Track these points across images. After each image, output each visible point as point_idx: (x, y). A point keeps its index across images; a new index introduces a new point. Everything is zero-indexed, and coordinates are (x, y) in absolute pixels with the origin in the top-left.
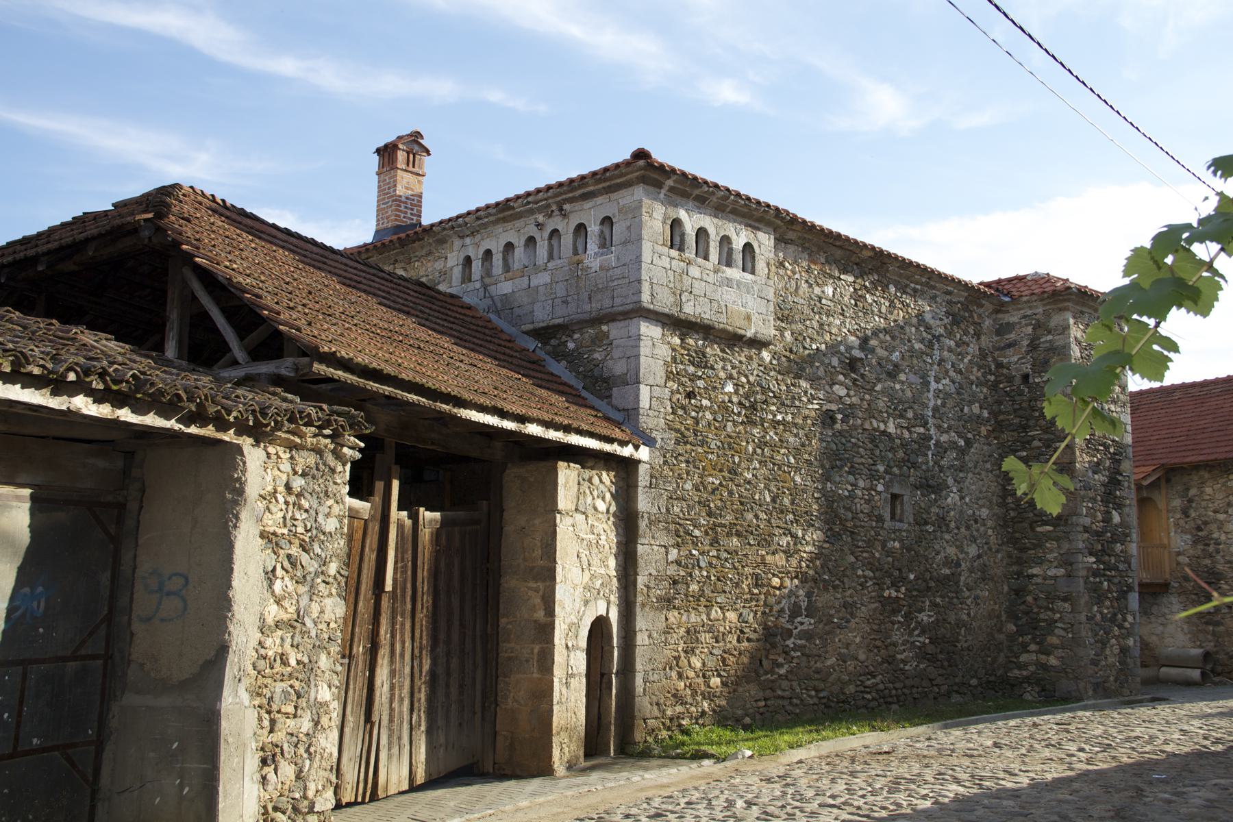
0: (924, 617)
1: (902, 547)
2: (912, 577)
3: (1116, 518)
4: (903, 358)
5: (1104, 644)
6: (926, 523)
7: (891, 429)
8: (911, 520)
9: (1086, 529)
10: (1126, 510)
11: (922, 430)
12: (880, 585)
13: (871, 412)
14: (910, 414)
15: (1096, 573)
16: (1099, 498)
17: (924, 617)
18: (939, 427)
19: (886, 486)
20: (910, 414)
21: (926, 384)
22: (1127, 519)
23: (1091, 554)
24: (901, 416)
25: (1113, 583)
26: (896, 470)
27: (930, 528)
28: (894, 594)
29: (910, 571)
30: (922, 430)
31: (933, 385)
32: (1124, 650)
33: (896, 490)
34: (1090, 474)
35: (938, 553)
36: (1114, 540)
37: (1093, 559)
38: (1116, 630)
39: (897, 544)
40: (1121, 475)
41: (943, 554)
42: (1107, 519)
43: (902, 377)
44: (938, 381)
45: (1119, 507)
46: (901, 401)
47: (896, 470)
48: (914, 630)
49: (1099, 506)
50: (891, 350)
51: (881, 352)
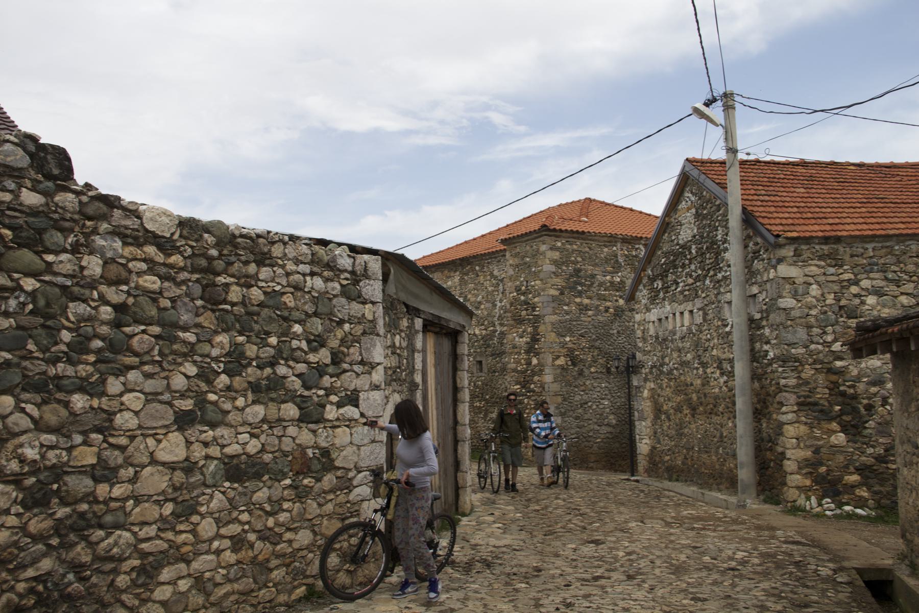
1: (483, 384)
2: (487, 397)
3: (535, 361)
4: (483, 298)
6: (494, 372)
7: (477, 332)
8: (486, 371)
9: (515, 370)
10: (542, 355)
11: (492, 328)
14: (486, 323)
16: (523, 351)
19: (474, 358)
20: (486, 323)
22: (542, 361)
24: (482, 325)
25: (533, 400)
26: (479, 350)
27: (497, 374)
28: (478, 405)
29: (487, 395)
30: (492, 328)
31: (499, 304)
33: (479, 359)
34: (517, 339)
35: (501, 385)
36: (534, 374)
37: (518, 387)
39: (480, 383)
40: (539, 335)
41: (503, 386)
42: (529, 363)
43: (482, 307)
44: (501, 301)
45: (537, 354)
46: (481, 318)
47: (479, 350)
48: (489, 420)
49: (524, 356)
50: (477, 296)
51: (473, 299)
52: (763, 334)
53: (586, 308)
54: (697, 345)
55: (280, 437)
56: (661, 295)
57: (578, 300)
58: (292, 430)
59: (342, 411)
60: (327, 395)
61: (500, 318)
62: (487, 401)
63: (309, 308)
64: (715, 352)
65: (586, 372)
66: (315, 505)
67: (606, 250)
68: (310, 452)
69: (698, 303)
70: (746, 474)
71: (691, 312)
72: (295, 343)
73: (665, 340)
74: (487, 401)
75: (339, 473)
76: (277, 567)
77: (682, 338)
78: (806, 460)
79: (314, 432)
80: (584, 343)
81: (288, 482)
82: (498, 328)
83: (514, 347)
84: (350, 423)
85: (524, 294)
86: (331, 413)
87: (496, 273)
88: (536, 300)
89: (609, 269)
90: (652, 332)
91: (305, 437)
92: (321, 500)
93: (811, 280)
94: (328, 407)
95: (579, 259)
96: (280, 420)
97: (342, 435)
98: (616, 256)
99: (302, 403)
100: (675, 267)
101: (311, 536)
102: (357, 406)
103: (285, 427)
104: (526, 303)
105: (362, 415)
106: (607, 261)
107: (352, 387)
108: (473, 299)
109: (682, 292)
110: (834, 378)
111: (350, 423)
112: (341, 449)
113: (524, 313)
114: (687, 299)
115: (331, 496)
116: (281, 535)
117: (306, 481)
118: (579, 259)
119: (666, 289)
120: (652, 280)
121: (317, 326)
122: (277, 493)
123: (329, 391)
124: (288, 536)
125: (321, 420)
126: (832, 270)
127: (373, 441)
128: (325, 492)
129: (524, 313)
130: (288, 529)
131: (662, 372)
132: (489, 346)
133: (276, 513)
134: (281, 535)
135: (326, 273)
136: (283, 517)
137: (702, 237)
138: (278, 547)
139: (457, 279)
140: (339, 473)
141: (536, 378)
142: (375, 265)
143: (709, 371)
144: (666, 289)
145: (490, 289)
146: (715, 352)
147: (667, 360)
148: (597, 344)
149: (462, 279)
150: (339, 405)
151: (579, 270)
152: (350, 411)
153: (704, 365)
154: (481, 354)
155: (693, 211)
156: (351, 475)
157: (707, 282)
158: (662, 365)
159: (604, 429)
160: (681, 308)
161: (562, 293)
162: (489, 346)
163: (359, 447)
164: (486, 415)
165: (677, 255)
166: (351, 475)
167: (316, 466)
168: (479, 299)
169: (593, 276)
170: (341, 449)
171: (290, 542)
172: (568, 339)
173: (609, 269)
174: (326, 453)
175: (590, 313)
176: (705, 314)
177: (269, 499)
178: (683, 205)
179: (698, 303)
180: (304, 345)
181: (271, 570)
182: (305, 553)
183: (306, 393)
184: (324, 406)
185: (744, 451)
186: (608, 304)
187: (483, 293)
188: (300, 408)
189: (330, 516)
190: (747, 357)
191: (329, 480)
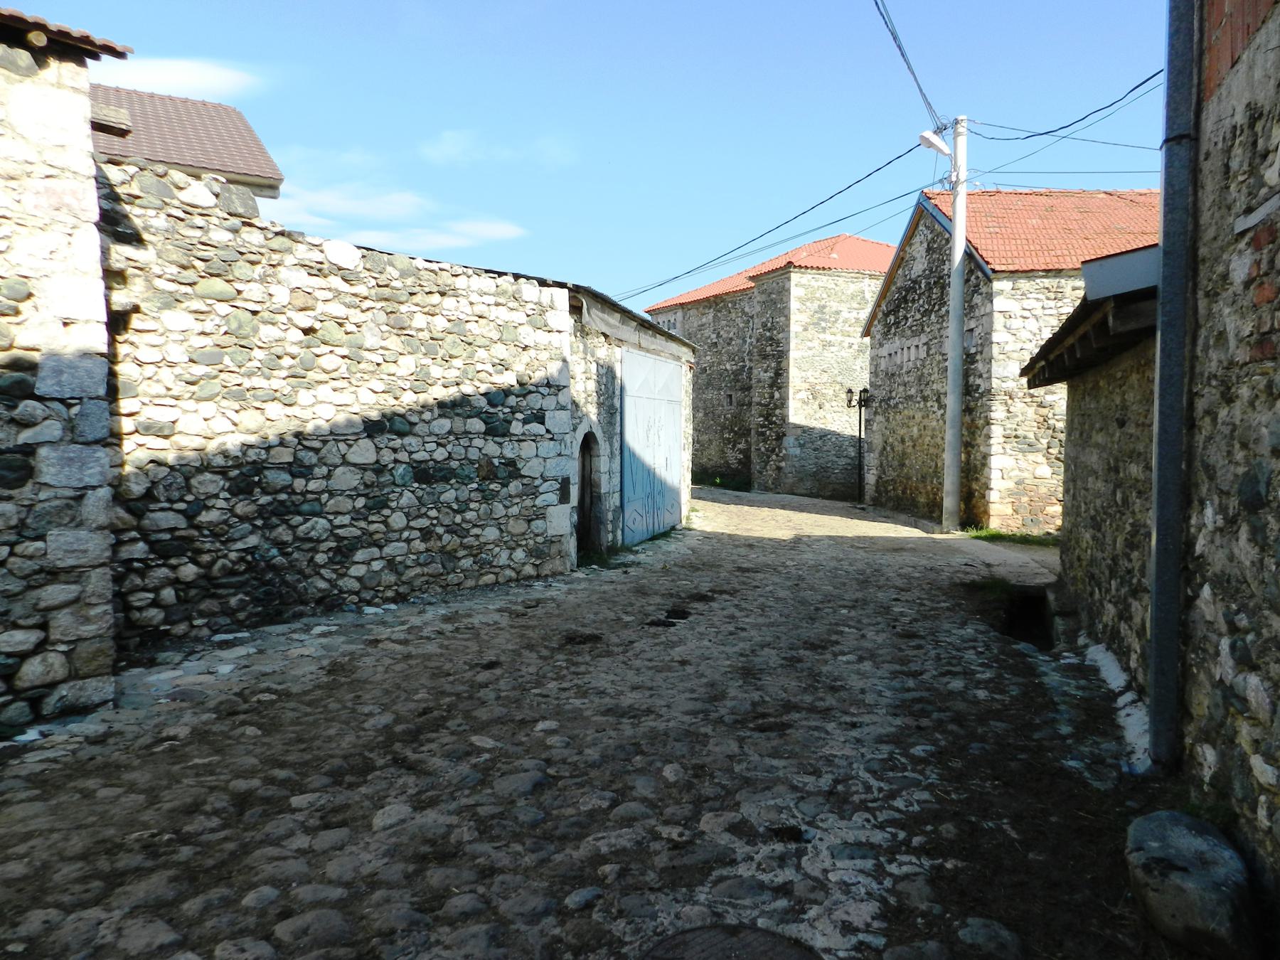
0: (740, 446)
3: (777, 395)
5: (767, 463)
7: (728, 367)
9: (759, 404)
12: (722, 431)
13: (719, 364)
15: (763, 426)
17: (740, 446)
18: (751, 360)
21: (745, 342)
23: (761, 416)
32: (779, 469)
36: (776, 407)
38: (774, 457)
42: (772, 397)
50: (729, 332)
51: (725, 335)
52: (976, 369)
53: (830, 344)
54: (920, 378)
55: (466, 448)
56: (893, 330)
57: (822, 336)
58: (478, 442)
59: (527, 427)
60: (513, 413)
61: (750, 353)
62: (736, 433)
63: (495, 335)
64: (935, 387)
65: (827, 406)
66: (501, 506)
67: (852, 286)
68: (496, 462)
69: (924, 338)
70: (949, 502)
71: (917, 346)
72: (479, 367)
73: (893, 375)
74: (736, 433)
75: (525, 481)
76: (464, 557)
77: (908, 372)
78: (1009, 490)
79: (500, 444)
80: (825, 377)
81: (475, 486)
82: (747, 363)
83: (759, 381)
84: (535, 438)
85: (769, 330)
86: (516, 428)
87: (747, 309)
88: (780, 336)
89: (856, 306)
90: (883, 367)
91: (491, 448)
92: (508, 504)
93: (1026, 314)
94: (514, 423)
95: (825, 296)
96: (467, 433)
97: (528, 449)
98: (863, 292)
99: (487, 418)
100: (906, 302)
101: (497, 532)
102: (543, 423)
103: (471, 439)
104: (771, 339)
105: (548, 431)
106: (853, 297)
107: (538, 406)
108: (725, 335)
109: (910, 328)
110: (1044, 411)
111: (535, 438)
112: (527, 460)
113: (768, 349)
114: (915, 334)
115: (517, 500)
116: (468, 531)
117: (492, 486)
118: (825, 296)
119: (897, 324)
120: (886, 315)
121: (500, 351)
122: (464, 494)
123: (514, 410)
124: (476, 531)
125: (506, 434)
126: (1052, 304)
127: (560, 455)
128: (510, 496)
129: (768, 349)
130: (475, 526)
131: (889, 406)
132: (738, 381)
133: (463, 511)
134: (468, 531)
135: (511, 305)
136: (470, 515)
137: (931, 271)
138: (465, 541)
139: (711, 316)
140: (525, 481)
141: (778, 412)
142: (562, 296)
143: (929, 404)
144: (897, 324)
145: (741, 325)
146: (935, 387)
147: (894, 394)
148: (839, 379)
149: (714, 317)
150: (525, 422)
151: (824, 307)
152: (535, 428)
153: (925, 399)
154: (731, 388)
155: (925, 245)
156: (537, 482)
157: (933, 317)
158: (890, 399)
159: (843, 461)
160: (908, 343)
161: (806, 329)
162: (738, 381)
163: (545, 459)
164: (734, 446)
165: (908, 290)
166: (537, 482)
167: (502, 473)
168: (731, 335)
169: (838, 313)
170: (527, 460)
171: (477, 536)
172: (809, 374)
173: (856, 306)
174: (511, 463)
175: (832, 349)
176: (929, 349)
177: (457, 499)
178: (917, 239)
179: (924, 338)
180: (489, 368)
181: (459, 559)
182: (491, 546)
183: (492, 410)
184: (510, 422)
185: (950, 482)
186: (851, 340)
187: (735, 330)
188: (486, 423)
189: (516, 517)
190: (959, 390)
191: (515, 486)
